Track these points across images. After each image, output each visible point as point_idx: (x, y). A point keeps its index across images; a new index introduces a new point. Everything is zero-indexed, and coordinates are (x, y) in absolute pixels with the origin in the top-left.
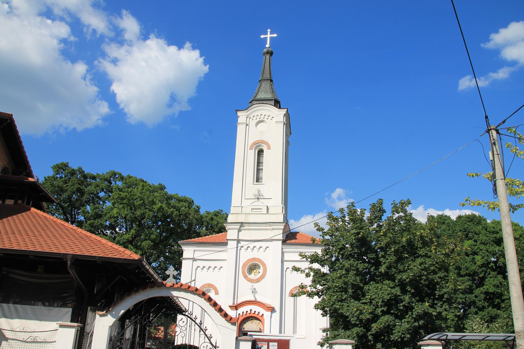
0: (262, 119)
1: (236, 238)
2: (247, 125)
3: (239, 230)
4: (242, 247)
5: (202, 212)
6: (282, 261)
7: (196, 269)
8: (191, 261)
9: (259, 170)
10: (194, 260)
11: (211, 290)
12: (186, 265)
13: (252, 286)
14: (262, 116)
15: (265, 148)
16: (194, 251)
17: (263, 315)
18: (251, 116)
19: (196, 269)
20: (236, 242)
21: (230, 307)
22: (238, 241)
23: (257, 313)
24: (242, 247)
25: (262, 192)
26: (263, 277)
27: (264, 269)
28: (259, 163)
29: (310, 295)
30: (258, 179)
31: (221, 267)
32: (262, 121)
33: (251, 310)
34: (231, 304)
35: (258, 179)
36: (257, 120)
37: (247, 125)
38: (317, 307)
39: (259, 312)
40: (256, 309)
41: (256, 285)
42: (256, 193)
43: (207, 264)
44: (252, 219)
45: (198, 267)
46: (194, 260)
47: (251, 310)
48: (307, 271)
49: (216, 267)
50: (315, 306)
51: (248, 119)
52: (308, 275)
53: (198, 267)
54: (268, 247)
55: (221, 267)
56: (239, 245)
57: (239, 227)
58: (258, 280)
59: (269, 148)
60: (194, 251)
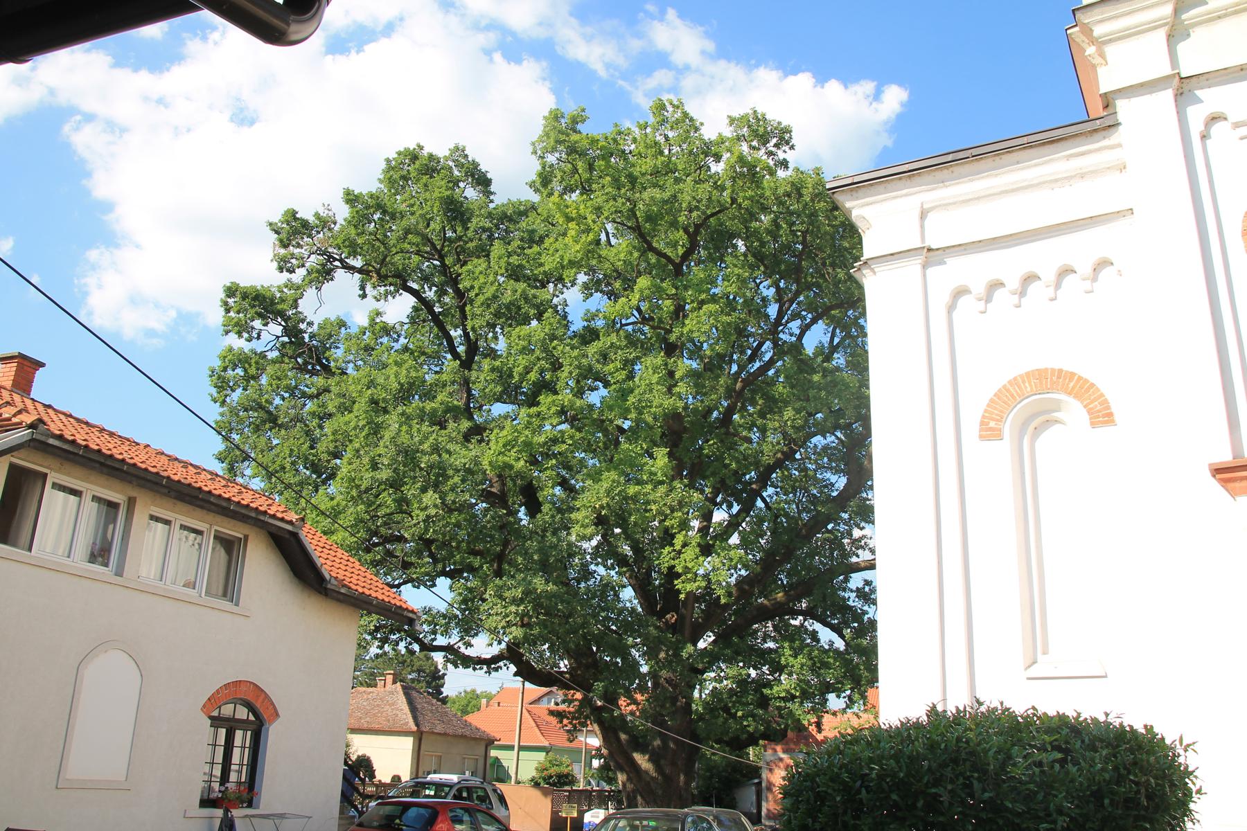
1: (1168, 71)
4: (1214, 119)
7: (951, 308)
8: (913, 267)
10: (931, 255)
11: (1058, 401)
12: (888, 297)
16: (923, 215)
19: (951, 308)
20: (1168, 95)
22: (1184, 88)
24: (1214, 119)
31: (1103, 264)
34: (1225, 456)
43: (1008, 265)
45: (960, 292)
46: (931, 255)
49: (1066, 271)
53: (960, 292)
55: (1103, 264)
56: (1196, 116)
60: (923, 215)
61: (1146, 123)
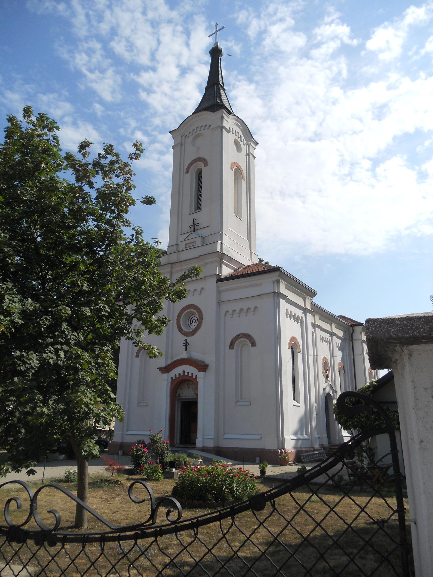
0: (198, 132)
6: (219, 303)
9: (199, 197)
13: (186, 340)
14: (199, 129)
17: (196, 376)
18: (187, 134)
21: (160, 369)
23: (190, 375)
25: (199, 221)
26: (198, 327)
33: (184, 371)
36: (193, 136)
39: (192, 374)
40: (190, 370)
41: (189, 339)
42: (192, 224)
47: (184, 371)
51: (184, 137)
54: (203, 288)
57: (170, 269)
58: (193, 333)
59: (206, 164)
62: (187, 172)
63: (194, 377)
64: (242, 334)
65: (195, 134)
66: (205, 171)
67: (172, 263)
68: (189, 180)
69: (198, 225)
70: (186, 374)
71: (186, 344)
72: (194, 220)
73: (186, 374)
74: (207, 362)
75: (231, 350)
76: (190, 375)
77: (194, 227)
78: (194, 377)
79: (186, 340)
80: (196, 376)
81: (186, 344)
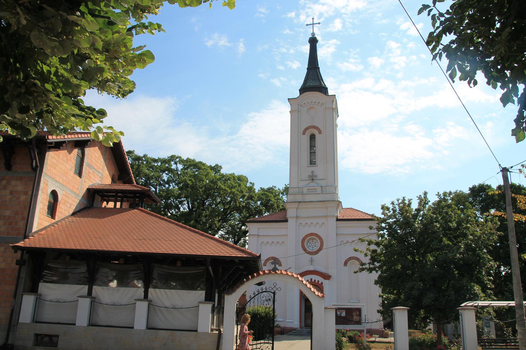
0: (312, 106)
2: (299, 112)
3: (297, 208)
5: (257, 188)
9: (312, 153)
13: (312, 258)
15: (316, 132)
23: (317, 282)
27: (321, 243)
28: (312, 146)
29: (370, 270)
30: (312, 163)
32: (311, 108)
35: (312, 163)
37: (299, 112)
38: (376, 283)
41: (315, 257)
44: (308, 198)
45: (262, 242)
48: (365, 251)
50: (375, 282)
52: (366, 255)
58: (316, 253)
59: (320, 132)
61: (291, 222)
62: (304, 133)
63: (320, 283)
64: (353, 257)
65: (308, 107)
66: (318, 137)
67: (300, 202)
68: (306, 139)
69: (316, 176)
70: (313, 281)
71: (312, 261)
72: (313, 172)
73: (313, 281)
74: (330, 274)
75: (345, 267)
76: (317, 282)
77: (312, 178)
78: (320, 283)
79: (312, 258)
80: (322, 283)
81: (312, 261)
